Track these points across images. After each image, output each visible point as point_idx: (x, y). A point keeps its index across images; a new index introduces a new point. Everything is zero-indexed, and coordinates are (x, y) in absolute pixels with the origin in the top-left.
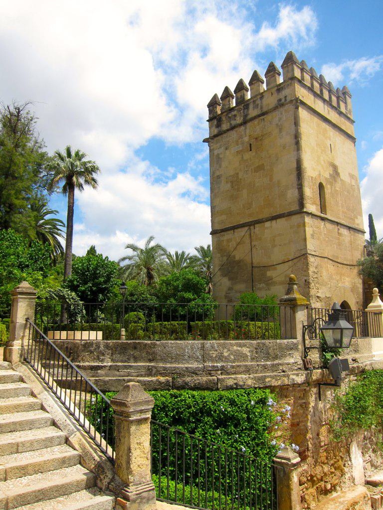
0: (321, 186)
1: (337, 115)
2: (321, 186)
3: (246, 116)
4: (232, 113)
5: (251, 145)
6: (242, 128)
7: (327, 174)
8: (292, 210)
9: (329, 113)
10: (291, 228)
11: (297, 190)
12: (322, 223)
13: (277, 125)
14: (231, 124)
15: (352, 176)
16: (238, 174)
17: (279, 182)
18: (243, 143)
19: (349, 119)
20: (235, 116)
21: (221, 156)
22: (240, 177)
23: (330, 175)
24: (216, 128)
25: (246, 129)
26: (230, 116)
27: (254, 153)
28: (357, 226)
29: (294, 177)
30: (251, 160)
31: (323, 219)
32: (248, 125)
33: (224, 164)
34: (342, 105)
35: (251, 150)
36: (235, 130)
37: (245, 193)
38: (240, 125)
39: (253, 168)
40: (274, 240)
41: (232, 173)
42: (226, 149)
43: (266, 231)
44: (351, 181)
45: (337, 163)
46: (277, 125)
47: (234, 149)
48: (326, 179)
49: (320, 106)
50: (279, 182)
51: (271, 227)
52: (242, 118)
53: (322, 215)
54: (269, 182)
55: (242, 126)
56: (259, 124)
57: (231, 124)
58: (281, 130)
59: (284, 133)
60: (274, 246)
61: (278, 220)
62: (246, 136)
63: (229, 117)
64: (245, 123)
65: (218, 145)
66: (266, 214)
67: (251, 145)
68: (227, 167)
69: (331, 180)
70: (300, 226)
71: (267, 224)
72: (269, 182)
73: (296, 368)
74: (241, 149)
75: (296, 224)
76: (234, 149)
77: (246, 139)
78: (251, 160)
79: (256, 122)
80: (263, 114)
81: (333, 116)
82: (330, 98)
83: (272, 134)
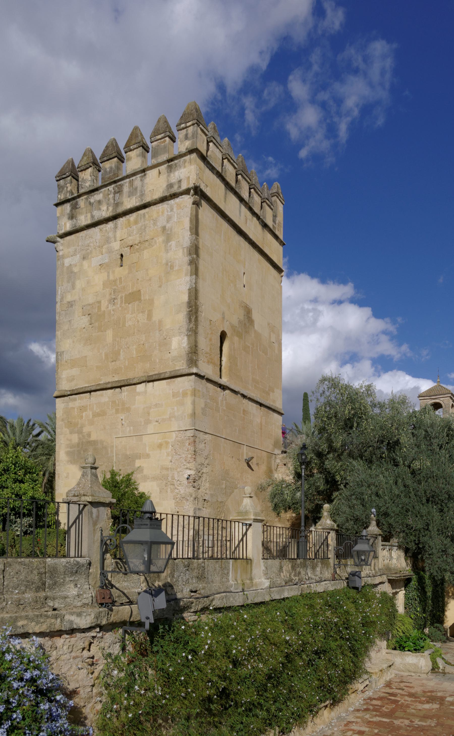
4: (95, 196)
5: (122, 255)
6: (111, 225)
7: (236, 317)
8: (177, 368)
10: (173, 396)
11: (186, 338)
13: (164, 228)
14: (92, 217)
16: (99, 302)
17: (160, 322)
18: (110, 251)
20: (99, 202)
22: (103, 308)
24: (69, 218)
25: (116, 227)
26: (92, 200)
27: (127, 272)
28: (271, 403)
29: (181, 317)
30: (121, 282)
33: (79, 284)
35: (121, 266)
36: (99, 227)
39: (124, 295)
40: (149, 414)
41: (91, 300)
42: (84, 258)
43: (137, 397)
46: (164, 228)
50: (160, 322)
51: (145, 392)
52: (111, 209)
54: (146, 321)
55: (111, 223)
57: (92, 217)
58: (168, 239)
61: (156, 383)
62: (115, 241)
63: (90, 203)
64: (115, 217)
65: (71, 250)
67: (122, 255)
68: (83, 289)
69: (240, 330)
70: (187, 394)
72: (146, 321)
73: (79, 604)
74: (107, 261)
75: (181, 391)
76: (96, 260)
77: (116, 245)
78: (121, 282)
79: (132, 217)
83: (156, 242)
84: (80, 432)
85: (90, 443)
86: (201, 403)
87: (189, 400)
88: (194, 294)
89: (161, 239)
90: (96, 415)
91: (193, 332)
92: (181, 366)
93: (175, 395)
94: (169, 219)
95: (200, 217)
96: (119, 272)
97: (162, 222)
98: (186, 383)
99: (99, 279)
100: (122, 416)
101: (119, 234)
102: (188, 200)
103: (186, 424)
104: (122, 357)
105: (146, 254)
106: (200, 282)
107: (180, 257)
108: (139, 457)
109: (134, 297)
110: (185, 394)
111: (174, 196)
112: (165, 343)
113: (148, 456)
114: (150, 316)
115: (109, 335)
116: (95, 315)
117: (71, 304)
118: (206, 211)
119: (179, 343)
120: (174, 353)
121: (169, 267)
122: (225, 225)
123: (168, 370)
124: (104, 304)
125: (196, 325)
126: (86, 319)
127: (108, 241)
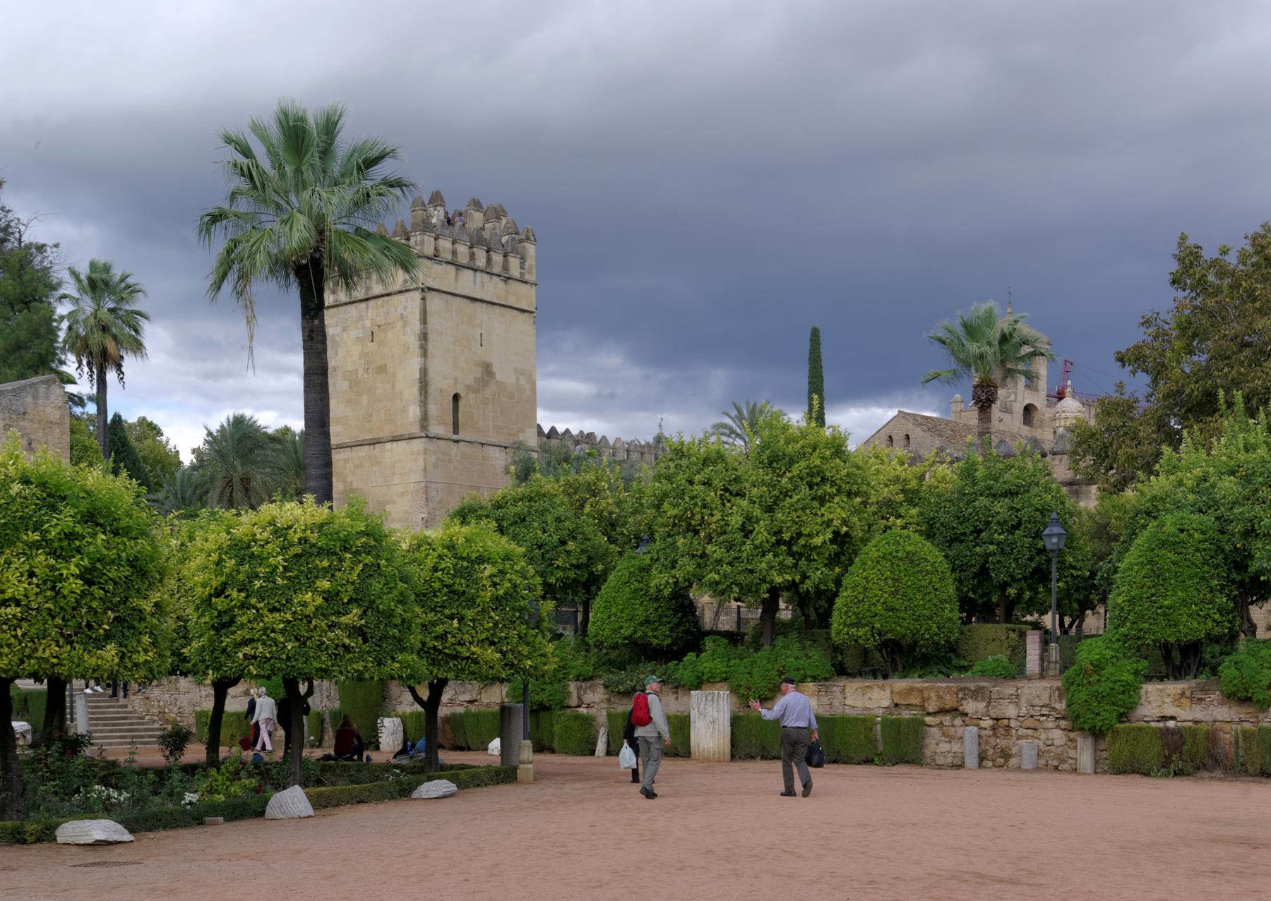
0: (456, 397)
1: (501, 285)
2: (456, 397)
3: (368, 289)
6: (363, 305)
9: (483, 285)
12: (454, 447)
15: (520, 372)
18: (364, 327)
19: (526, 282)
21: (338, 339)
23: (476, 379)
29: (415, 390)
31: (457, 441)
32: (372, 302)
33: (341, 352)
34: (514, 262)
37: (365, 398)
38: (361, 301)
41: (350, 367)
44: (518, 380)
45: (487, 360)
47: (354, 333)
48: (468, 387)
49: (468, 283)
53: (455, 437)
56: (382, 306)
58: (405, 326)
59: (408, 329)
60: (394, 474)
64: (367, 300)
66: (385, 433)
71: (388, 445)
76: (354, 333)
77: (368, 323)
80: (388, 295)
81: (491, 288)
82: (489, 260)
84: (345, 481)
85: (353, 491)
86: (433, 459)
87: (421, 458)
88: (424, 372)
89: (400, 324)
90: (356, 467)
91: (424, 403)
92: (415, 430)
93: (412, 453)
94: (405, 308)
95: (428, 308)
96: (371, 347)
97: (400, 310)
98: (418, 445)
99: (356, 350)
100: (375, 469)
101: (371, 313)
102: (417, 296)
103: (419, 477)
104: (374, 419)
105: (390, 334)
106: (429, 360)
107: (414, 342)
108: (388, 503)
109: (382, 369)
110: (419, 453)
111: (408, 291)
112: (404, 411)
113: (394, 502)
114: (393, 387)
115: (365, 398)
116: (354, 382)
117: (335, 369)
118: (435, 302)
119: (414, 411)
120: (411, 419)
121: (406, 347)
122: (458, 299)
123: (407, 432)
124: (360, 372)
125: (426, 398)
126: (346, 384)
127: (361, 318)
